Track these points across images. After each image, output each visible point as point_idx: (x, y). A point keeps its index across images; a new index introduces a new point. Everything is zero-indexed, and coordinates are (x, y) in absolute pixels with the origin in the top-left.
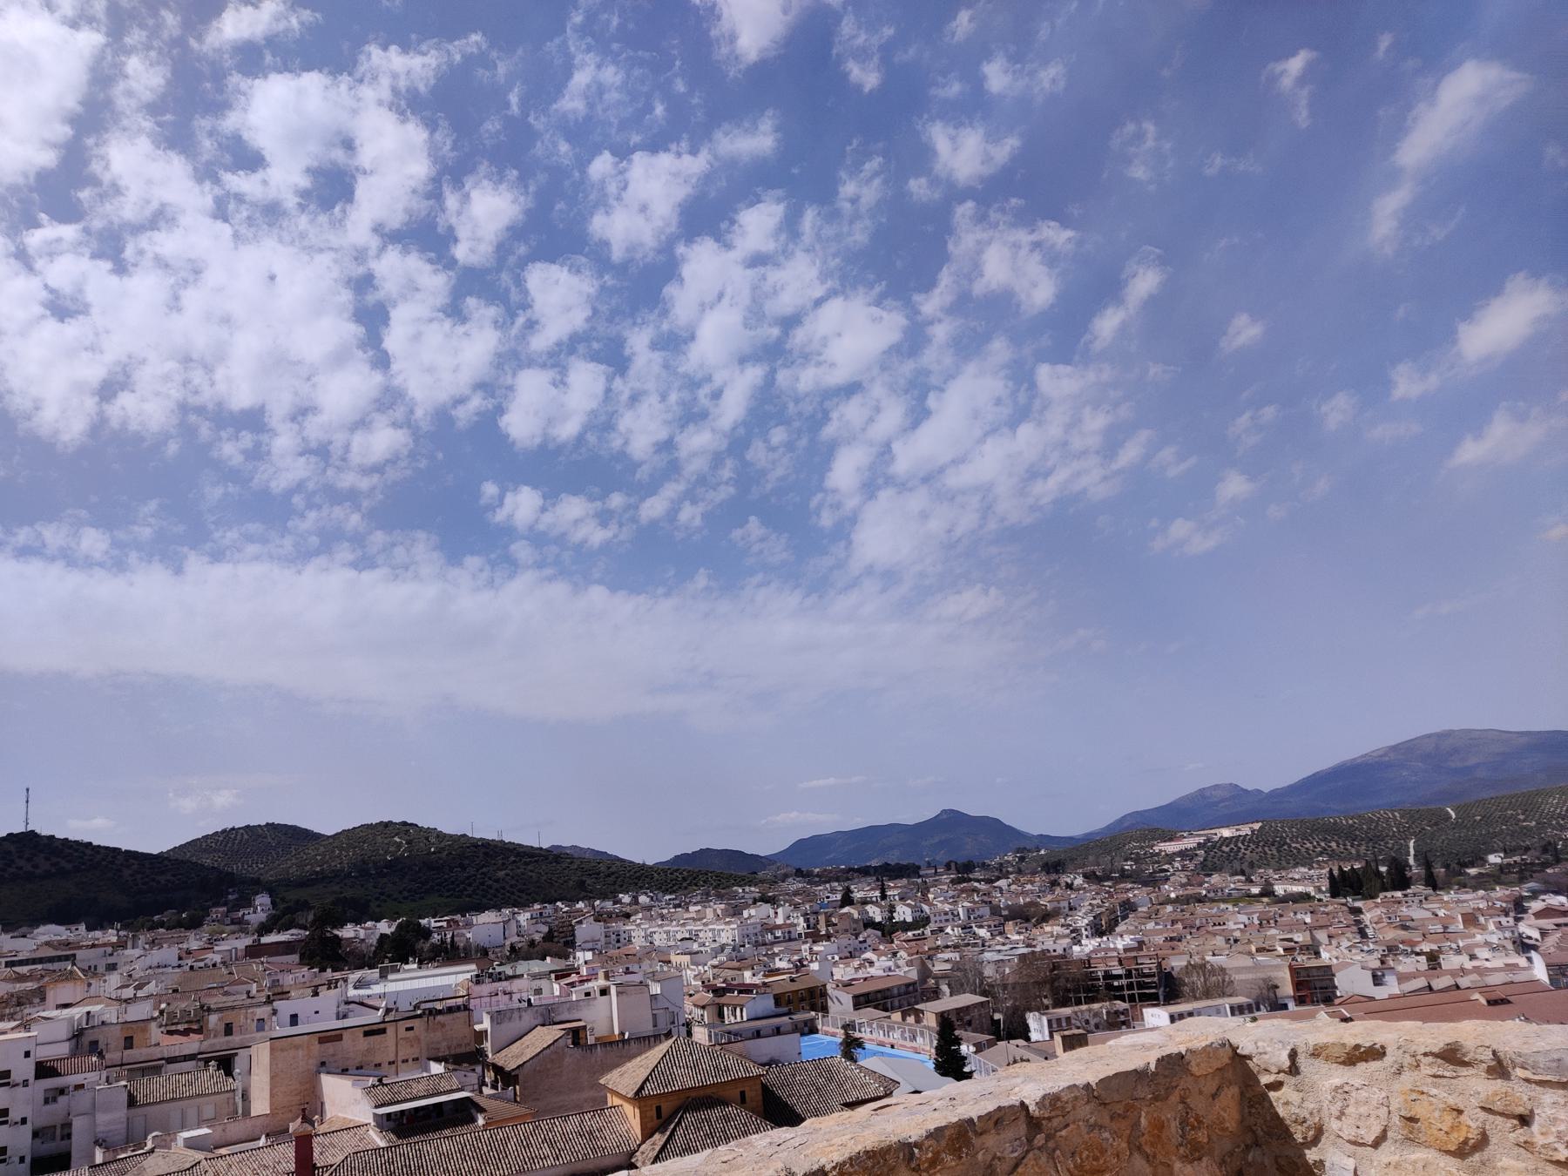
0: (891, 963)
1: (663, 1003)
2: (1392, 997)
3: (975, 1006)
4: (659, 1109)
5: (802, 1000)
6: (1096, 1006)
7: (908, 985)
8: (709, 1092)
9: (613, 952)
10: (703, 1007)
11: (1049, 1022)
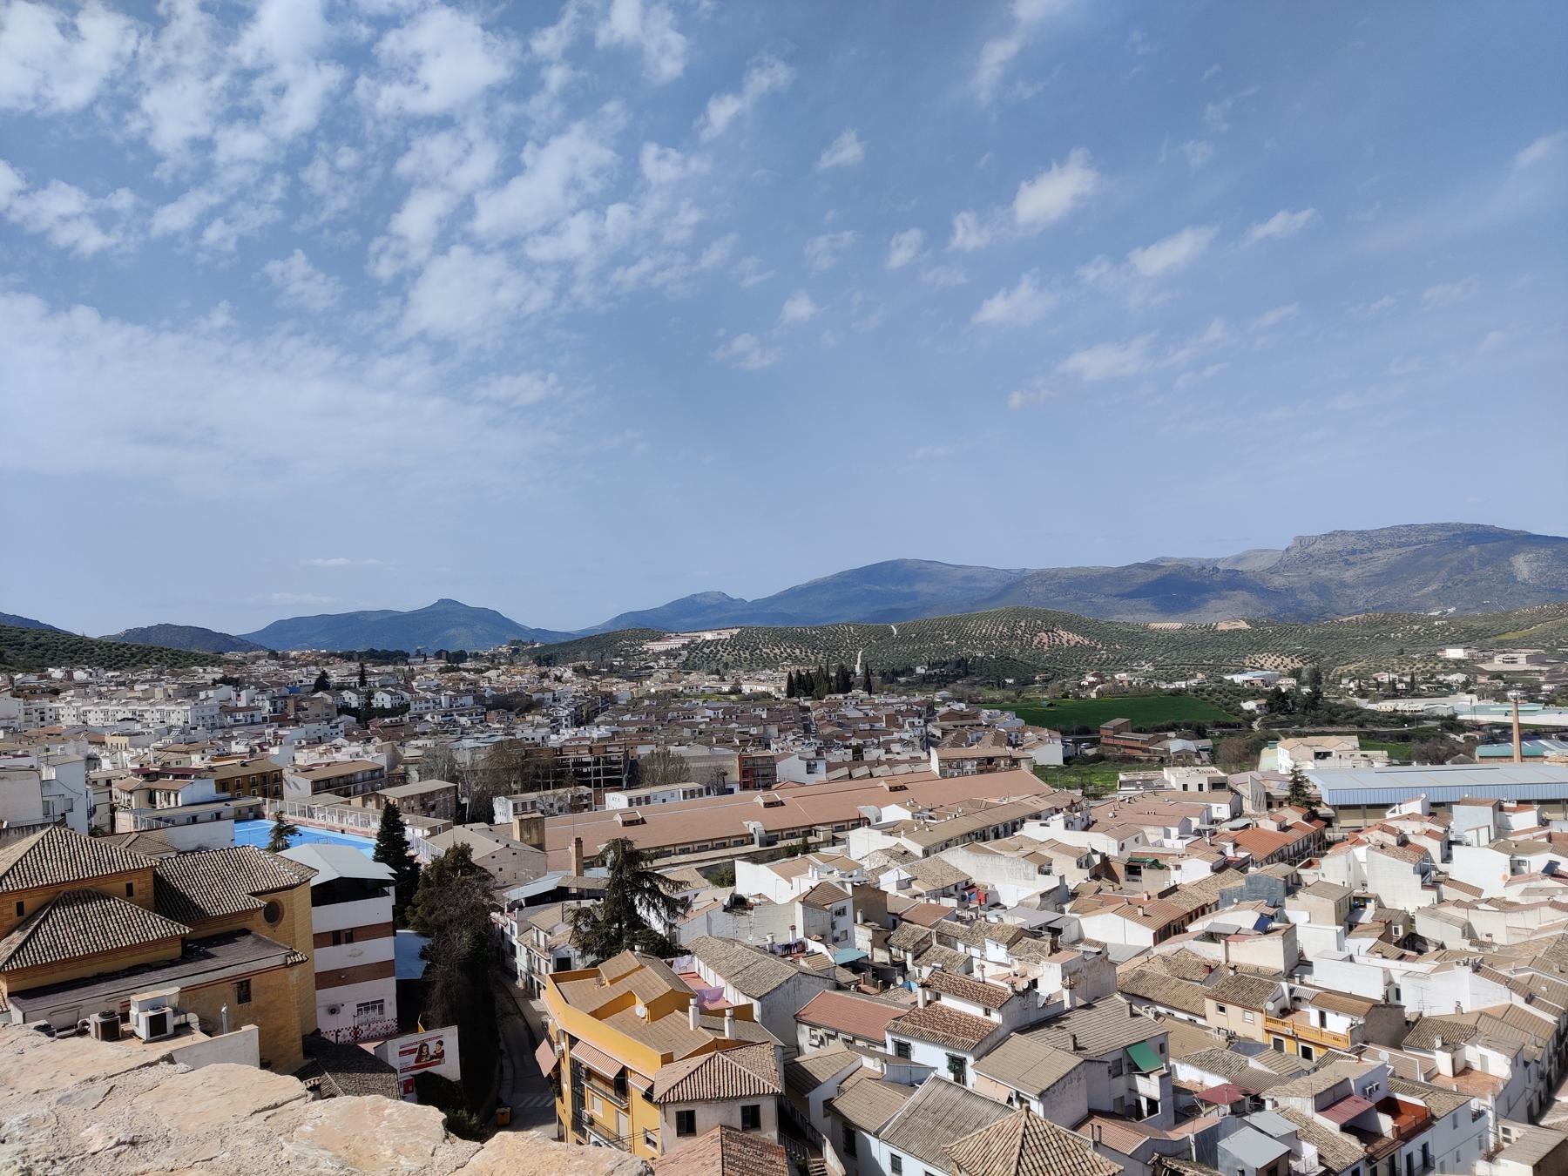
0: (359, 749)
1: (56, 790)
2: (820, 784)
3: (440, 791)
4: (20, 906)
5: (254, 785)
6: (561, 791)
7: (373, 771)
8: (87, 885)
9: (32, 730)
10: (131, 792)
11: (515, 806)
